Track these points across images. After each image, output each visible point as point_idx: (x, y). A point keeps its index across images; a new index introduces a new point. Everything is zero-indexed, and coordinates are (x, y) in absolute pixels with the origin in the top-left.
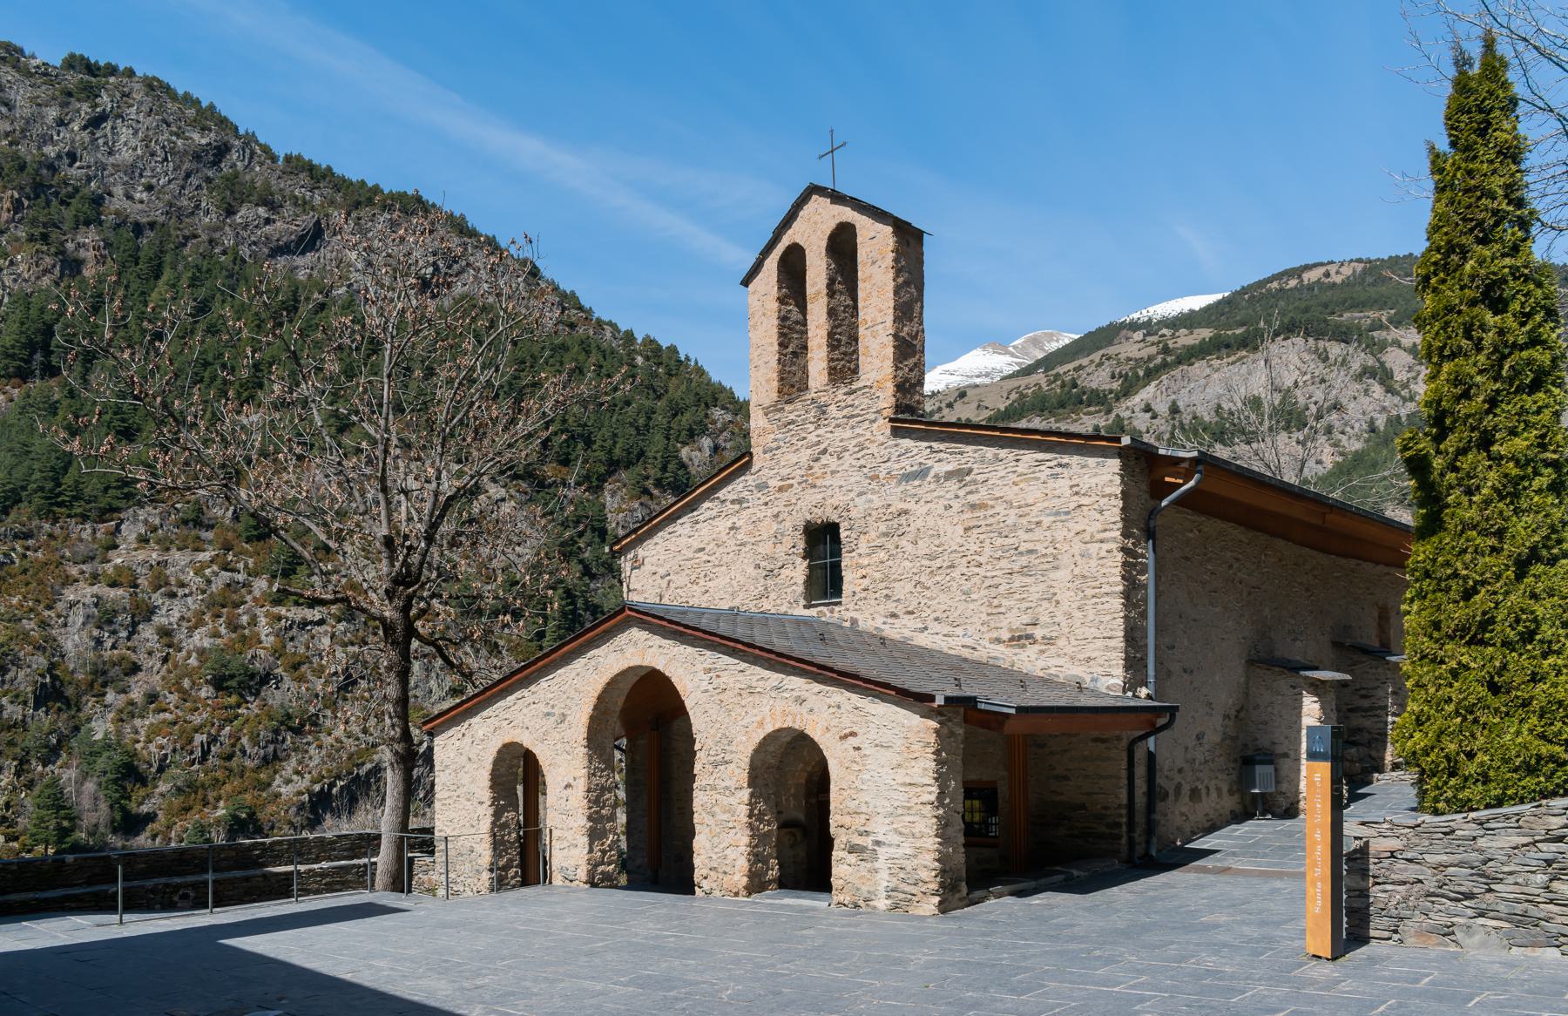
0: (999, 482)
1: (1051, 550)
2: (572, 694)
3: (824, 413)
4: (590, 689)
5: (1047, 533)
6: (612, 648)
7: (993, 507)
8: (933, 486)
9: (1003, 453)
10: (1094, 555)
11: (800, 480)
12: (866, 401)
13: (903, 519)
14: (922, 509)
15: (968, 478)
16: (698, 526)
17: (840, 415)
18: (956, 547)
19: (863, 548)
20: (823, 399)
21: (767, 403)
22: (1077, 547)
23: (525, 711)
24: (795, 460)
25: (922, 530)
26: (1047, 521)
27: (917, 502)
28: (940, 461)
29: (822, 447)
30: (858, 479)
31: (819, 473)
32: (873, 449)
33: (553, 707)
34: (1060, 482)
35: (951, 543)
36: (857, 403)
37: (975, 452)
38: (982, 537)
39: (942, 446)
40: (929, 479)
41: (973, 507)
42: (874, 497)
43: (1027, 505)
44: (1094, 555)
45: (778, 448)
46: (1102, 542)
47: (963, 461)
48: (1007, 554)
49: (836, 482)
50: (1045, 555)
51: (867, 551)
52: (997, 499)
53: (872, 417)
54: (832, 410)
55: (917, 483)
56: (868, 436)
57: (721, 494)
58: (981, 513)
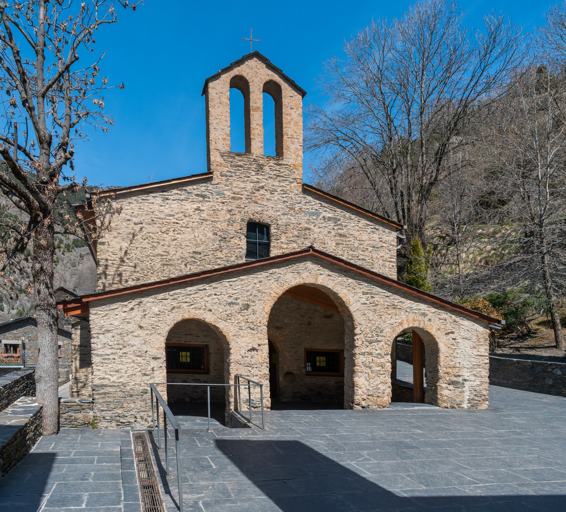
0: (351, 228)
1: (371, 261)
2: (255, 292)
3: (262, 168)
4: (272, 292)
5: (370, 254)
6: (289, 270)
7: (349, 237)
8: (322, 221)
9: (353, 217)
10: (387, 266)
11: (247, 197)
12: (287, 171)
13: (307, 232)
14: (318, 230)
15: (339, 223)
16: (168, 201)
17: (271, 172)
18: (332, 250)
19: (283, 239)
20: (262, 162)
21: (223, 150)
22: (381, 262)
23: (207, 299)
24: (242, 185)
25: (317, 239)
26: (370, 249)
27: (314, 226)
28: (325, 211)
29: (261, 185)
30: (283, 207)
31: (259, 197)
32: (292, 195)
33: (236, 299)
34: (375, 235)
35: (330, 248)
36: (282, 170)
37: (342, 212)
38: (344, 249)
39: (326, 205)
40: (320, 217)
41: (341, 235)
42: (292, 218)
43: (363, 241)
44: (387, 266)
45: (232, 176)
46: (390, 262)
47: (336, 215)
48: (354, 258)
49: (270, 204)
50: (368, 262)
51: (286, 242)
52: (351, 235)
53: (292, 180)
54: (266, 168)
55: (315, 217)
56: (288, 188)
57: (188, 188)
58: (344, 239)
